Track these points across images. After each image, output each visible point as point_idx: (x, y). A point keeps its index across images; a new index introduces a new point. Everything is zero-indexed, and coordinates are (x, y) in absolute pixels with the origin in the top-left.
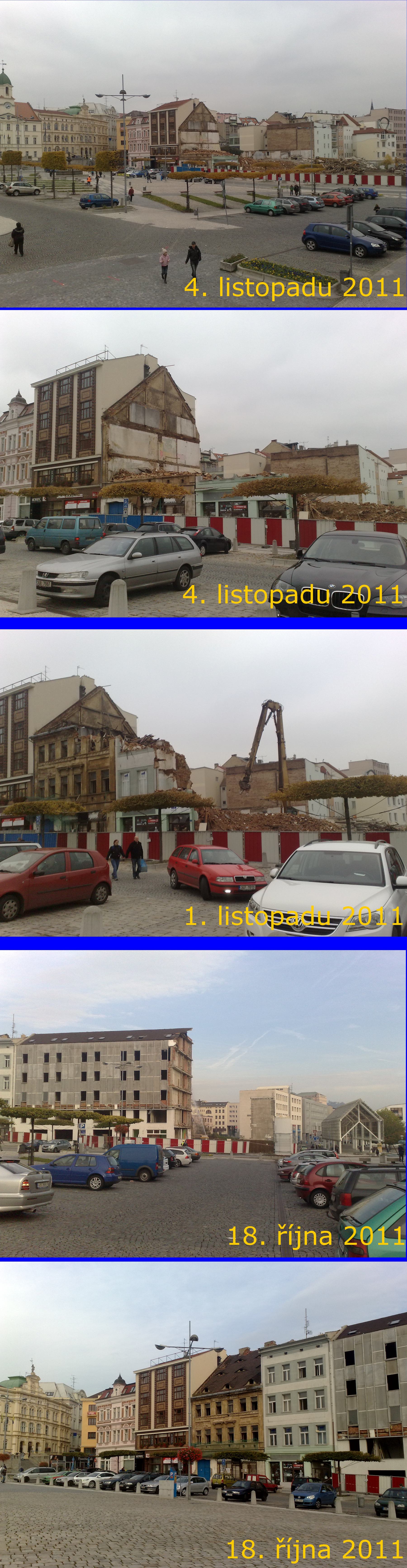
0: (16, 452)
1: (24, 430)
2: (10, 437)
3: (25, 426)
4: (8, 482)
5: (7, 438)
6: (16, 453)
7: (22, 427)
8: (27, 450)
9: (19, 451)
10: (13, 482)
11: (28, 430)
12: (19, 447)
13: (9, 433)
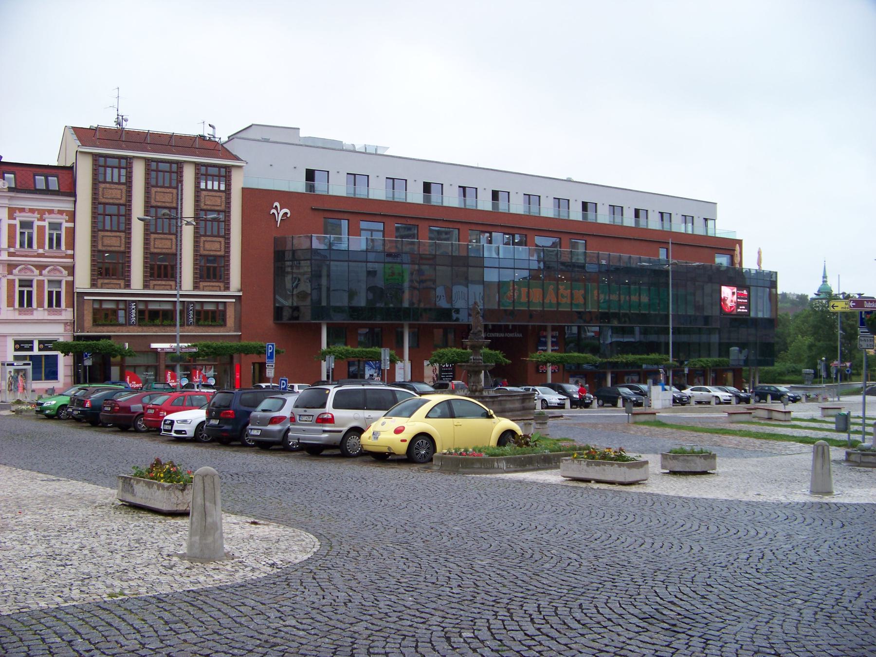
9: (10, 254)
11: (41, 219)
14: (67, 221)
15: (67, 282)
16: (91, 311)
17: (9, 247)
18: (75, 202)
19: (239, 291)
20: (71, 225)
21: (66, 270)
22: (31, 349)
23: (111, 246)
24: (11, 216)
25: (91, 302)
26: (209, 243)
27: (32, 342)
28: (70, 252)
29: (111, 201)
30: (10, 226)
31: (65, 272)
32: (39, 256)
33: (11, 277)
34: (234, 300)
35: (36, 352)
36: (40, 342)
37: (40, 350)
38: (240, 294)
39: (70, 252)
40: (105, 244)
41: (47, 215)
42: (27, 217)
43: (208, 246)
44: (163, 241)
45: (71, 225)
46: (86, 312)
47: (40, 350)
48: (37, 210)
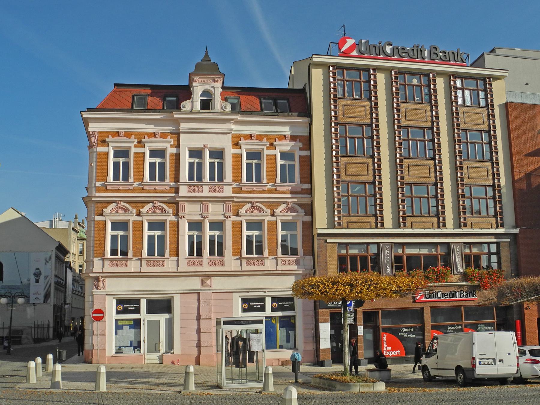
0: (228, 192)
6: (228, 192)
14: (301, 149)
15: (304, 223)
16: (336, 258)
17: (234, 181)
18: (310, 124)
19: (516, 227)
20: (306, 153)
21: (302, 209)
22: (263, 309)
23: (357, 175)
24: (236, 145)
25: (336, 245)
26: (474, 170)
27: (263, 300)
28: (307, 186)
29: (354, 121)
30: (234, 156)
31: (302, 211)
32: (269, 191)
34: (509, 240)
35: (269, 312)
36: (274, 300)
37: (273, 310)
38: (516, 231)
39: (307, 186)
40: (349, 172)
41: (277, 142)
42: (254, 146)
43: (473, 173)
44: (420, 168)
45: (306, 153)
46: (329, 260)
47: (273, 310)
48: (267, 136)
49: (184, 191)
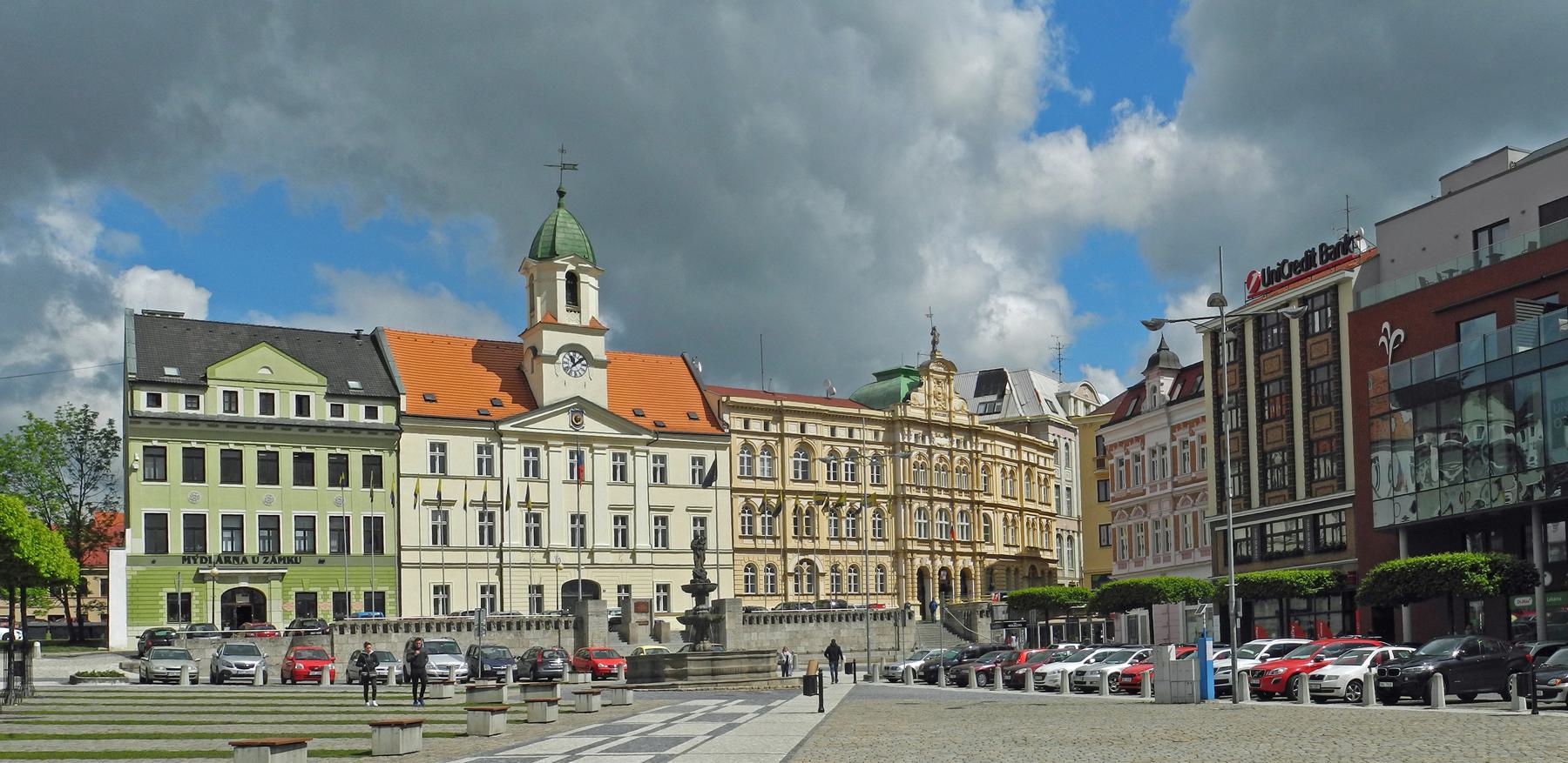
1: (1183, 434)
2: (1154, 452)
3: (1185, 424)
4: (1156, 561)
5: (1145, 453)
7: (1178, 427)
8: (1194, 481)
9: (1175, 485)
10: (1167, 559)
12: (1174, 474)
13: (1150, 442)
24: (1173, 439)
33: (1176, 513)
49: (1148, 494)
